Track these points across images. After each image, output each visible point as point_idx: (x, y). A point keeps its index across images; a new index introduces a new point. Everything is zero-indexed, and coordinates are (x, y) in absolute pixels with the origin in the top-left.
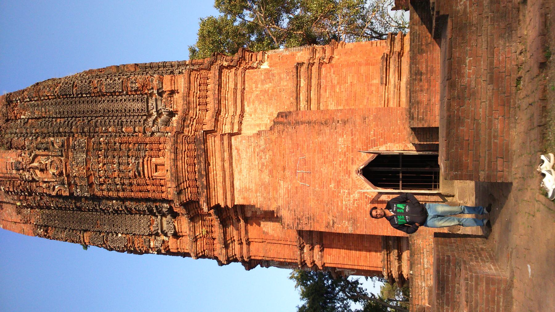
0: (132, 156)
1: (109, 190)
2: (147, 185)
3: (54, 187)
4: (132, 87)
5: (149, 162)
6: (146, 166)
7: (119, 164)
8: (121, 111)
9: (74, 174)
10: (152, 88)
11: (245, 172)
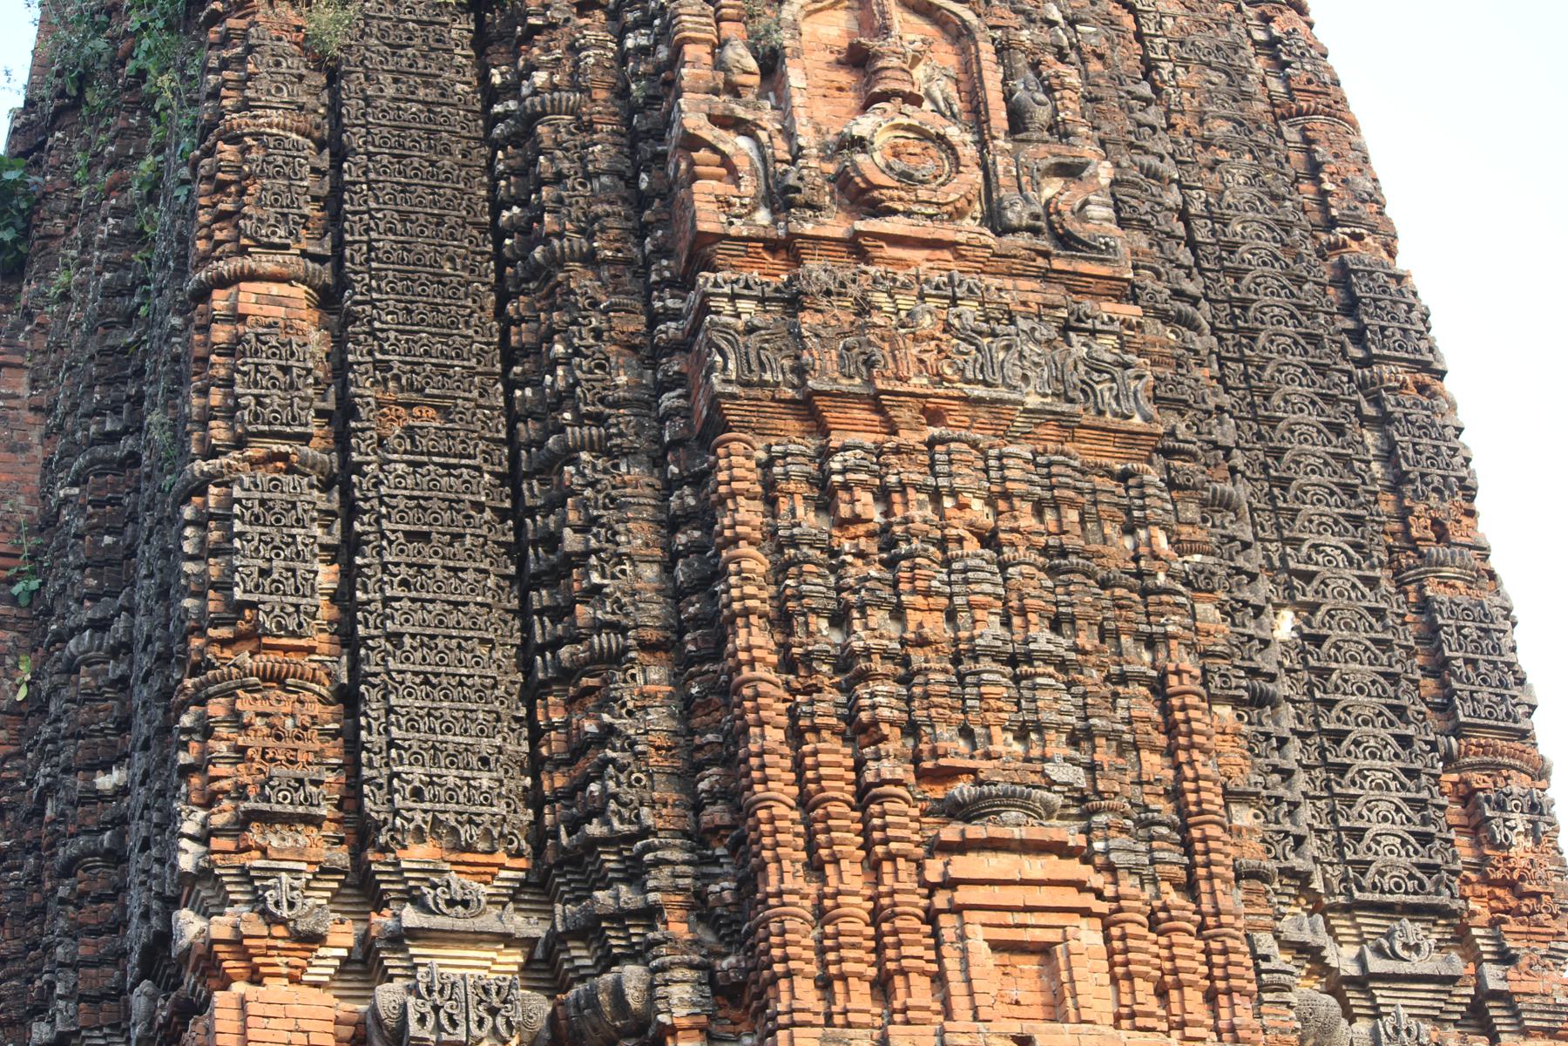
0: (1091, 768)
1: (778, 543)
2: (873, 867)
4: (1501, 806)
5: (1071, 898)
6: (1036, 867)
7: (1013, 661)
8: (1330, 704)
9: (880, 298)
10: (1506, 958)
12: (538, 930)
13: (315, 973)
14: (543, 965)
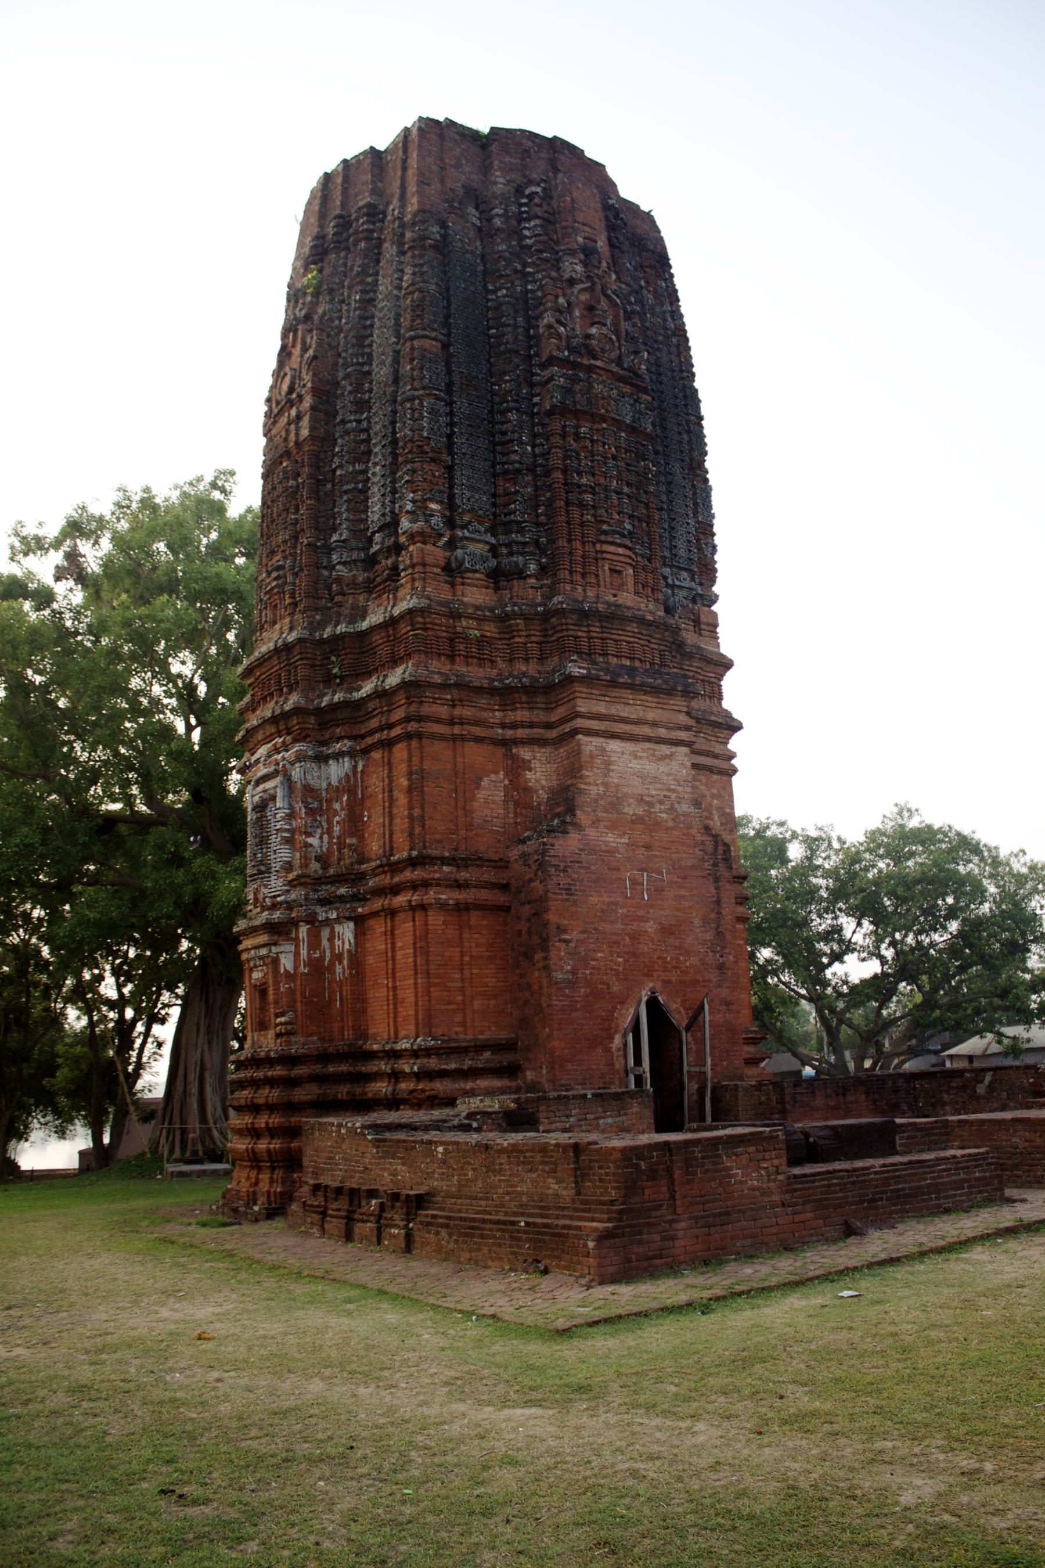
3: (564, 326)
6: (621, 551)
11: (635, 765)
12: (494, 541)
13: (440, 544)
14: (494, 550)
